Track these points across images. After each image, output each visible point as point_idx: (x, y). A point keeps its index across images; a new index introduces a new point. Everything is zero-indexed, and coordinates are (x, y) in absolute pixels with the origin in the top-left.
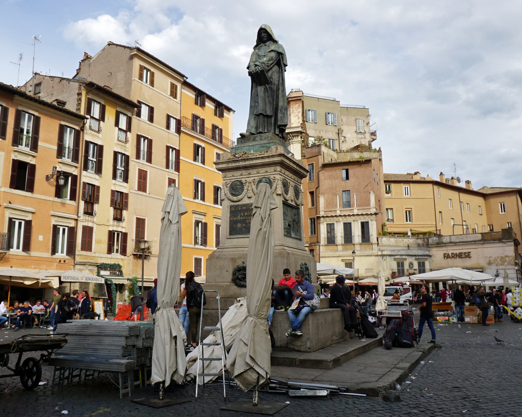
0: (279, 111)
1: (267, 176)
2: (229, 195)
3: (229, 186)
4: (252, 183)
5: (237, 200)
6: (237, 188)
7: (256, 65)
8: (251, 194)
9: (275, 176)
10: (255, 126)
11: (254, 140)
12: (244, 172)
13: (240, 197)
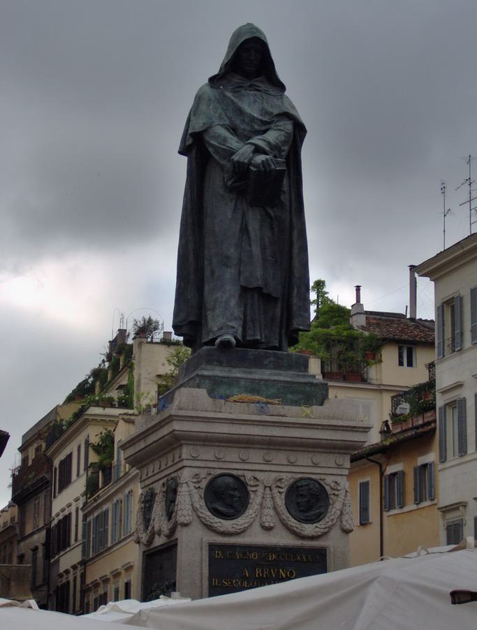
1: (313, 477)
2: (207, 514)
3: (204, 484)
4: (275, 491)
5: (231, 530)
6: (232, 496)
7: (258, 150)
8: (270, 519)
9: (339, 479)
10: (242, 316)
11: (258, 363)
12: (256, 456)
13: (241, 522)
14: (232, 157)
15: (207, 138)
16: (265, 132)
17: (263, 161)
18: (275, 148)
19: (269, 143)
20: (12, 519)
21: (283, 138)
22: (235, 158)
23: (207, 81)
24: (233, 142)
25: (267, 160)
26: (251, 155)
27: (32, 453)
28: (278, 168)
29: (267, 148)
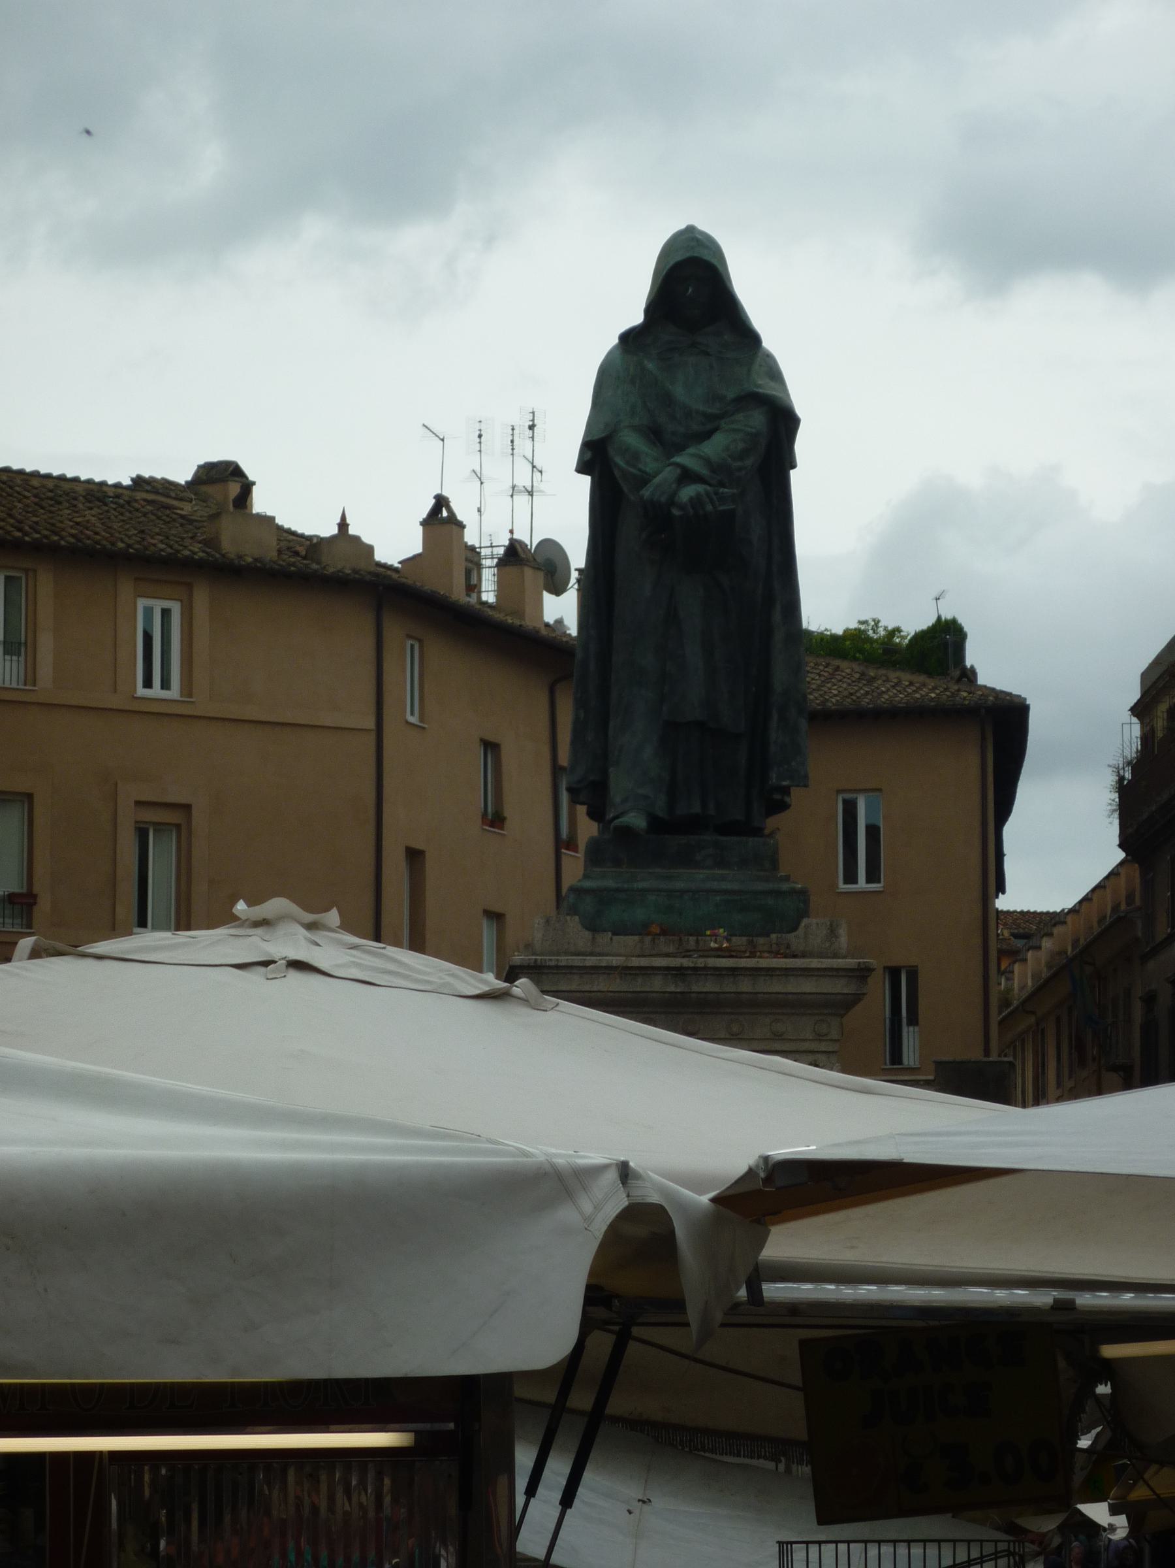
0: (775, 716)
7: (687, 476)
14: (641, 493)
15: (611, 452)
16: (708, 435)
17: (691, 499)
18: (720, 471)
19: (707, 461)
20: (1130, 898)
21: (741, 446)
22: (646, 493)
23: (616, 341)
24: (650, 458)
25: (698, 495)
26: (674, 486)
27: (1160, 723)
28: (721, 508)
29: (705, 472)
